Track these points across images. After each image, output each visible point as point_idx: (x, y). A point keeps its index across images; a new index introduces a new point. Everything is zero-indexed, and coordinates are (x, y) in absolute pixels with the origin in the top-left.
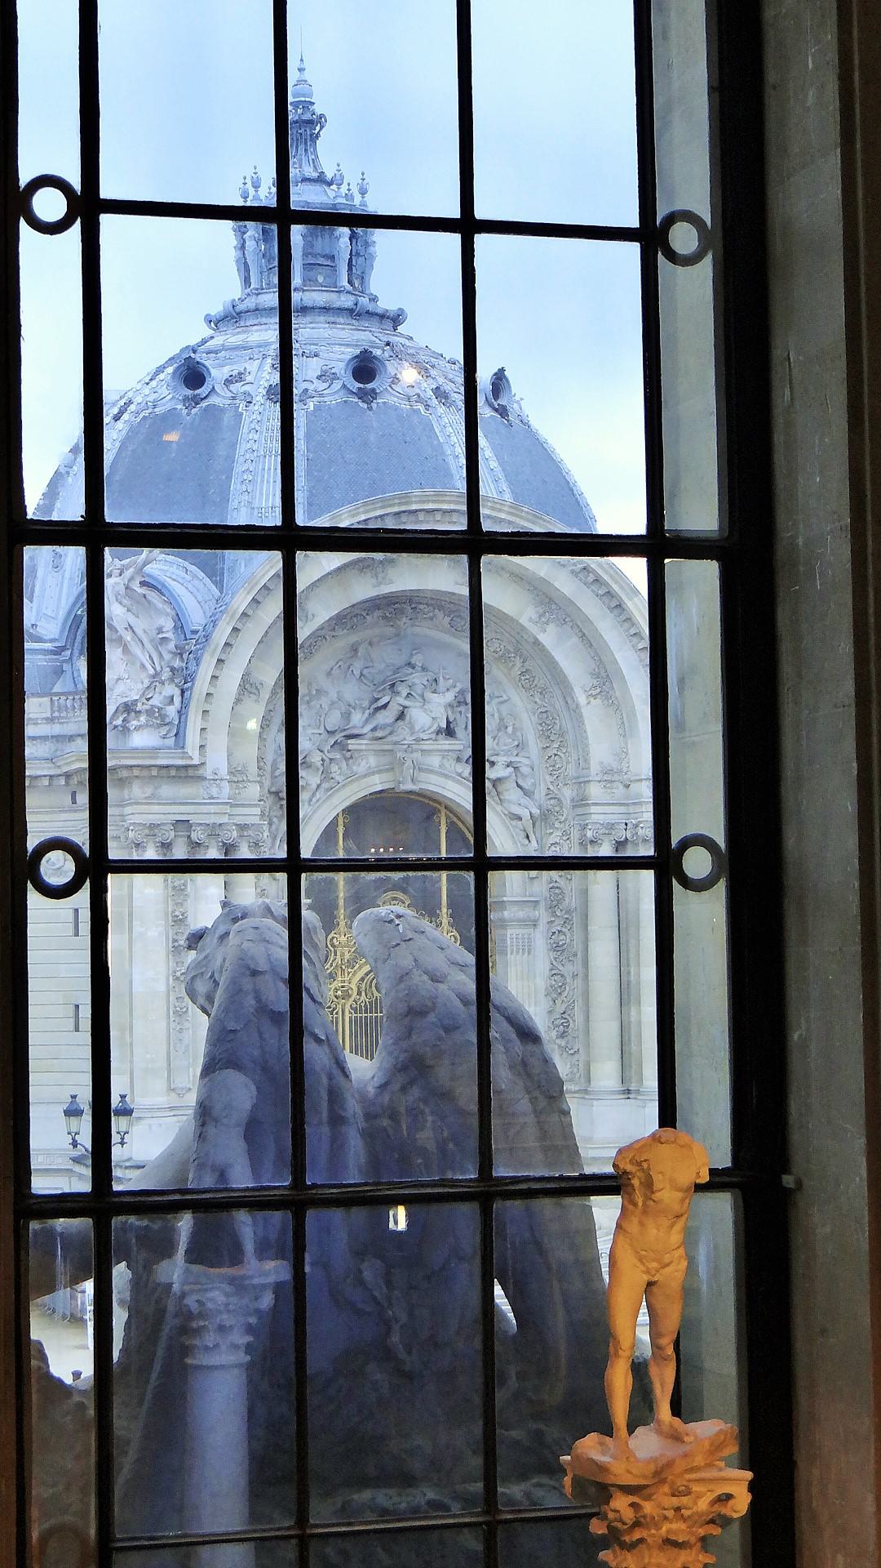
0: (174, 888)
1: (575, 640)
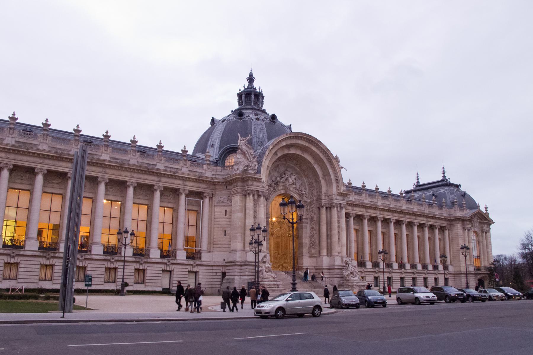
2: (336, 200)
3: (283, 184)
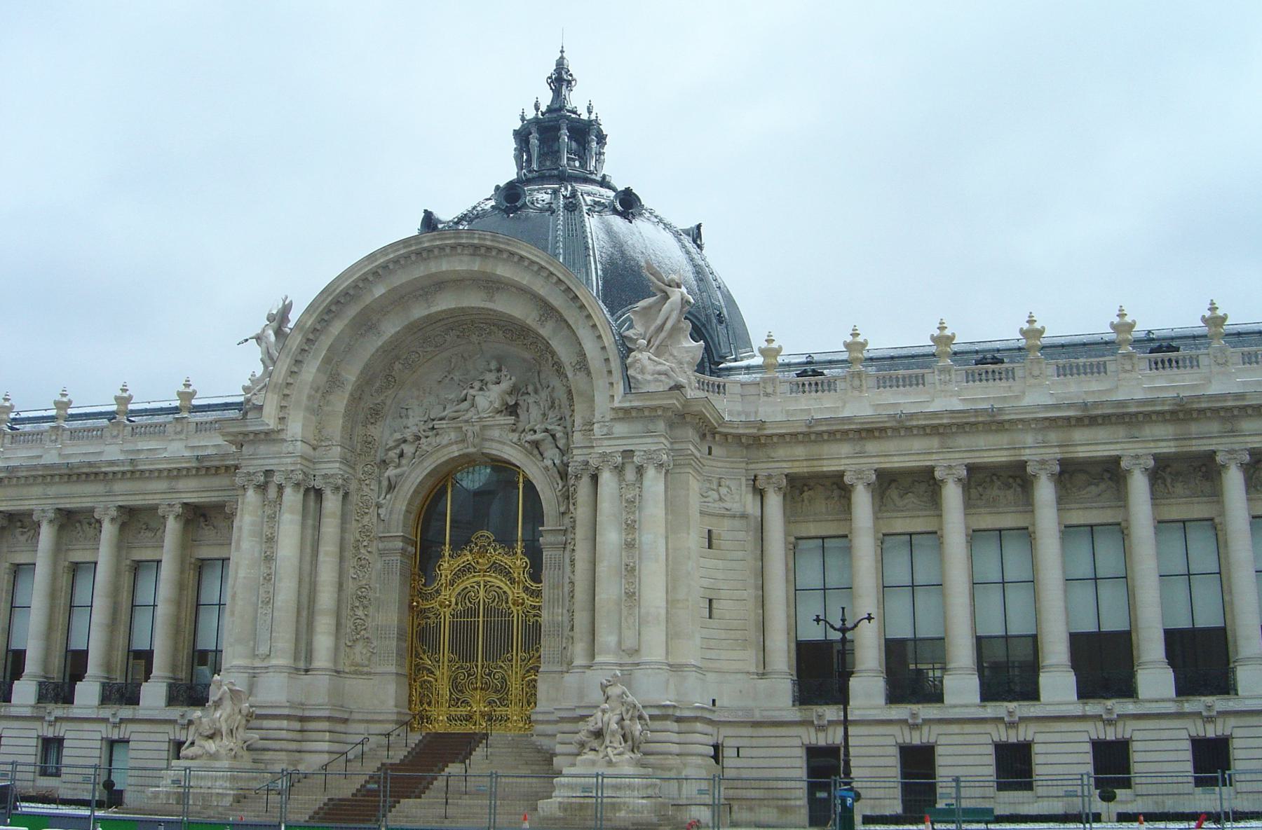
1: (566, 332)
2: (606, 443)
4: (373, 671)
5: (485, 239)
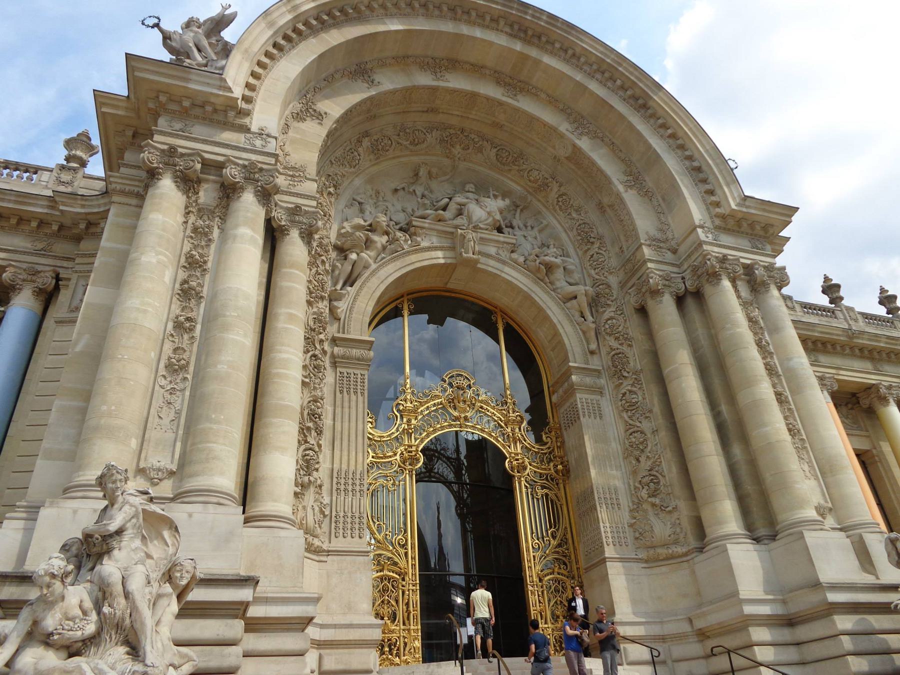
0: (195, 230)
3: (440, 226)
4: (325, 547)
5: (539, 19)
